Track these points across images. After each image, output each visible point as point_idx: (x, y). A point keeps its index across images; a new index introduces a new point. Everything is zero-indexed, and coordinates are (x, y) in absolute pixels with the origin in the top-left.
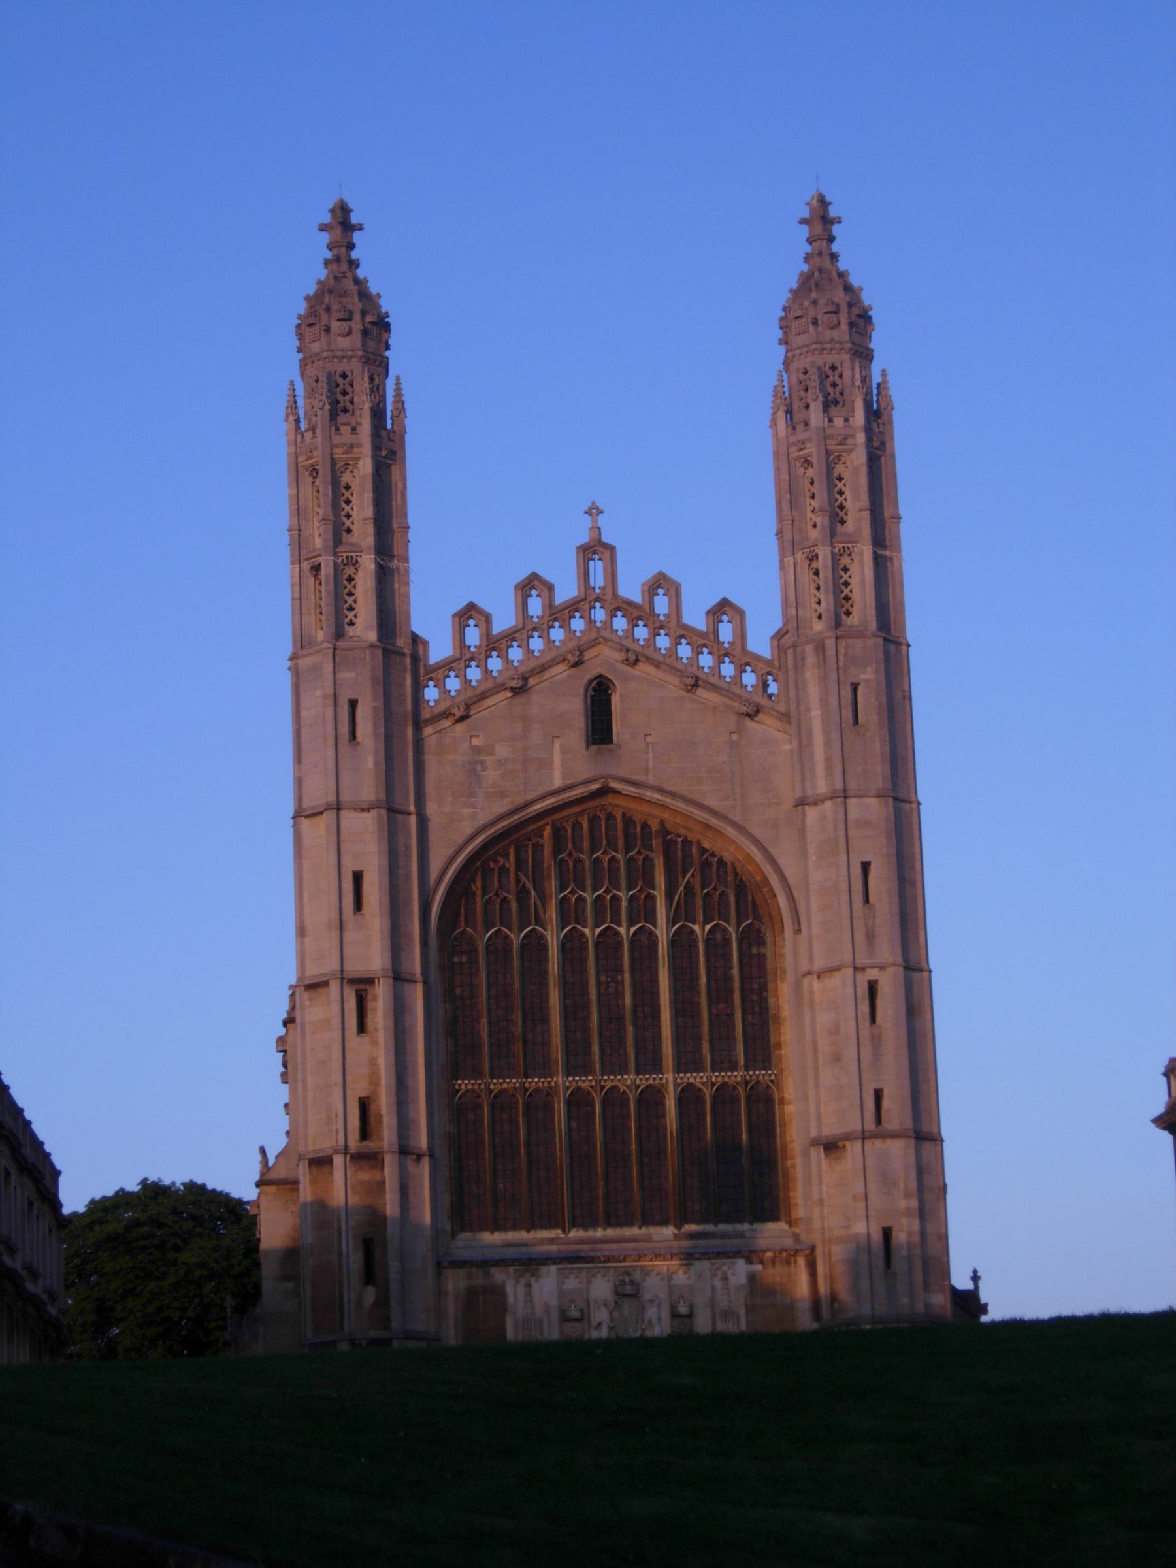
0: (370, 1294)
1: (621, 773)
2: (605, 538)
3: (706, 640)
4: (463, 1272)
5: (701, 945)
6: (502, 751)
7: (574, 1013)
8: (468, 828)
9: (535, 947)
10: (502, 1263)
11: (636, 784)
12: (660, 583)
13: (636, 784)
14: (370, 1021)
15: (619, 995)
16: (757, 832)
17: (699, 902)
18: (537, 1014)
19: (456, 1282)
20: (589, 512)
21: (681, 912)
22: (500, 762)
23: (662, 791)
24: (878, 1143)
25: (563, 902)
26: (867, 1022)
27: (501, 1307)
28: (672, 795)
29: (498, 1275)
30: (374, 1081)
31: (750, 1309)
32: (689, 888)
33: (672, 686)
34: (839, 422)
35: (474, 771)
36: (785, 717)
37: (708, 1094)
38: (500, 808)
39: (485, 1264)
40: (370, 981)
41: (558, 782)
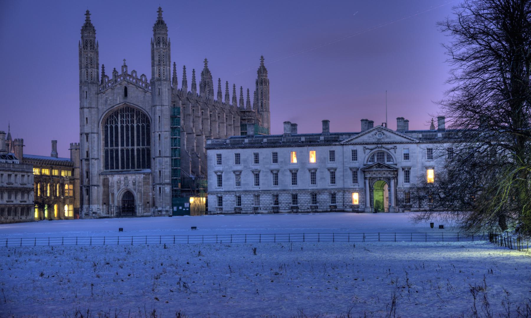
0: (87, 180)
1: (127, 101)
2: (126, 65)
3: (141, 80)
4: (103, 176)
5: (141, 127)
6: (110, 98)
8: (105, 110)
9: (117, 127)
11: (130, 103)
12: (134, 71)
13: (130, 103)
15: (128, 134)
16: (147, 110)
17: (140, 120)
19: (102, 177)
20: (124, 60)
21: (138, 122)
22: (110, 100)
23: (133, 104)
24: (159, 158)
25: (121, 120)
26: (159, 140)
27: (109, 181)
28: (135, 105)
29: (108, 176)
30: (89, 149)
31: (144, 182)
32: (139, 118)
34: (158, 47)
37: (141, 149)
38: (111, 106)
40: (88, 134)
41: (118, 103)
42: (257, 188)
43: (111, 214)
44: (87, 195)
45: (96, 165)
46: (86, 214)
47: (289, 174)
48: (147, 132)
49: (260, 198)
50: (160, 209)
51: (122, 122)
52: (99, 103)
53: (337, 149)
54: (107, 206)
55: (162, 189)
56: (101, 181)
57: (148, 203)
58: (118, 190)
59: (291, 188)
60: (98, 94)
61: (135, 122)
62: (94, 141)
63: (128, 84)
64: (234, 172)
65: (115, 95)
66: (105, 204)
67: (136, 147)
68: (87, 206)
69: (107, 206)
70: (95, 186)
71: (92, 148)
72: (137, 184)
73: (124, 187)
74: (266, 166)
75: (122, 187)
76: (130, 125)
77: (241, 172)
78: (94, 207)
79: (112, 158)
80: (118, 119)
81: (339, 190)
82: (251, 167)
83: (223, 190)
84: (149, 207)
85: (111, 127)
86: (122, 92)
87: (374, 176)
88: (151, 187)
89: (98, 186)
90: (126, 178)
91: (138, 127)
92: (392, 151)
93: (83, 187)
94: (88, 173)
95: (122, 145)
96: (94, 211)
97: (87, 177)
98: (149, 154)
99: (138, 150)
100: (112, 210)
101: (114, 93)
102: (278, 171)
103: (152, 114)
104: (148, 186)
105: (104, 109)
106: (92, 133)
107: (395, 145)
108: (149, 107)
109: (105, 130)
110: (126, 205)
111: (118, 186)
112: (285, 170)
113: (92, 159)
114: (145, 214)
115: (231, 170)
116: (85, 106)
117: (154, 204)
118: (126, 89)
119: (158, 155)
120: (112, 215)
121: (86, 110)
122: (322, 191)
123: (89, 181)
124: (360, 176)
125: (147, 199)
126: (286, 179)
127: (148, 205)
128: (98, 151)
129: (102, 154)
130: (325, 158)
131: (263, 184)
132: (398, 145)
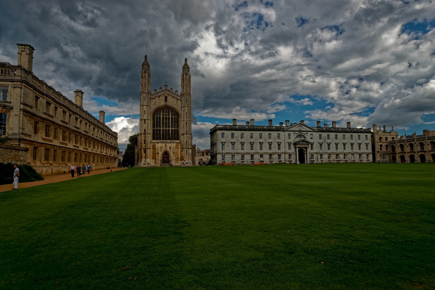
3: (175, 94)
6: (157, 102)
7: (163, 123)
8: (154, 108)
9: (160, 118)
10: (156, 143)
12: (171, 89)
14: (146, 123)
15: (166, 122)
16: (178, 109)
18: (160, 123)
19: (152, 144)
27: (156, 146)
29: (155, 144)
30: (146, 128)
31: (176, 147)
32: (173, 113)
33: (172, 97)
35: (155, 103)
36: (181, 100)
38: (157, 106)
39: (154, 143)
41: (162, 104)
42: (242, 151)
43: (157, 164)
44: (144, 153)
45: (149, 137)
46: (144, 164)
47: (259, 144)
48: (177, 121)
49: (245, 157)
50: (187, 162)
51: (163, 115)
52: (151, 104)
53: (282, 133)
54: (155, 160)
55: (188, 151)
56: (151, 146)
57: (178, 158)
58: (161, 151)
59: (260, 152)
60: (151, 99)
61: (170, 115)
62: (149, 124)
63: (168, 95)
64: (231, 143)
65: (160, 100)
66: (153, 158)
67: (170, 129)
68: (145, 159)
69: (155, 160)
70: (149, 148)
71: (148, 128)
72: (172, 148)
73: (164, 150)
74: (247, 140)
75: (163, 150)
76: (167, 117)
77: (235, 143)
78: (148, 160)
79: (157, 134)
80: (161, 114)
81: (282, 153)
82: (240, 140)
83: (225, 152)
84: (179, 161)
85: (157, 118)
86: (164, 98)
87: (301, 146)
88: (180, 150)
89: (150, 149)
90: (166, 146)
91: (172, 118)
92: (306, 135)
93: (142, 149)
94: (144, 141)
95: (163, 127)
96: (148, 162)
97: (145, 143)
98: (178, 133)
99: (172, 130)
100: (158, 162)
101: (160, 99)
102: (254, 143)
103: (181, 111)
104: (178, 149)
105: (154, 107)
106: (148, 119)
107: (307, 132)
108: (179, 108)
109: (153, 119)
110: (166, 159)
111: (161, 149)
112: (257, 142)
113: (148, 133)
114: (177, 165)
115: (229, 142)
116: (144, 105)
117: (182, 159)
118: (166, 97)
119: (185, 133)
120: (158, 165)
121: (145, 107)
122: (274, 153)
123: (146, 145)
124: (292, 147)
125: (178, 156)
126: (257, 147)
127: (178, 159)
128: (150, 129)
129: (152, 131)
130: (276, 137)
131: (246, 149)
132: (308, 132)
